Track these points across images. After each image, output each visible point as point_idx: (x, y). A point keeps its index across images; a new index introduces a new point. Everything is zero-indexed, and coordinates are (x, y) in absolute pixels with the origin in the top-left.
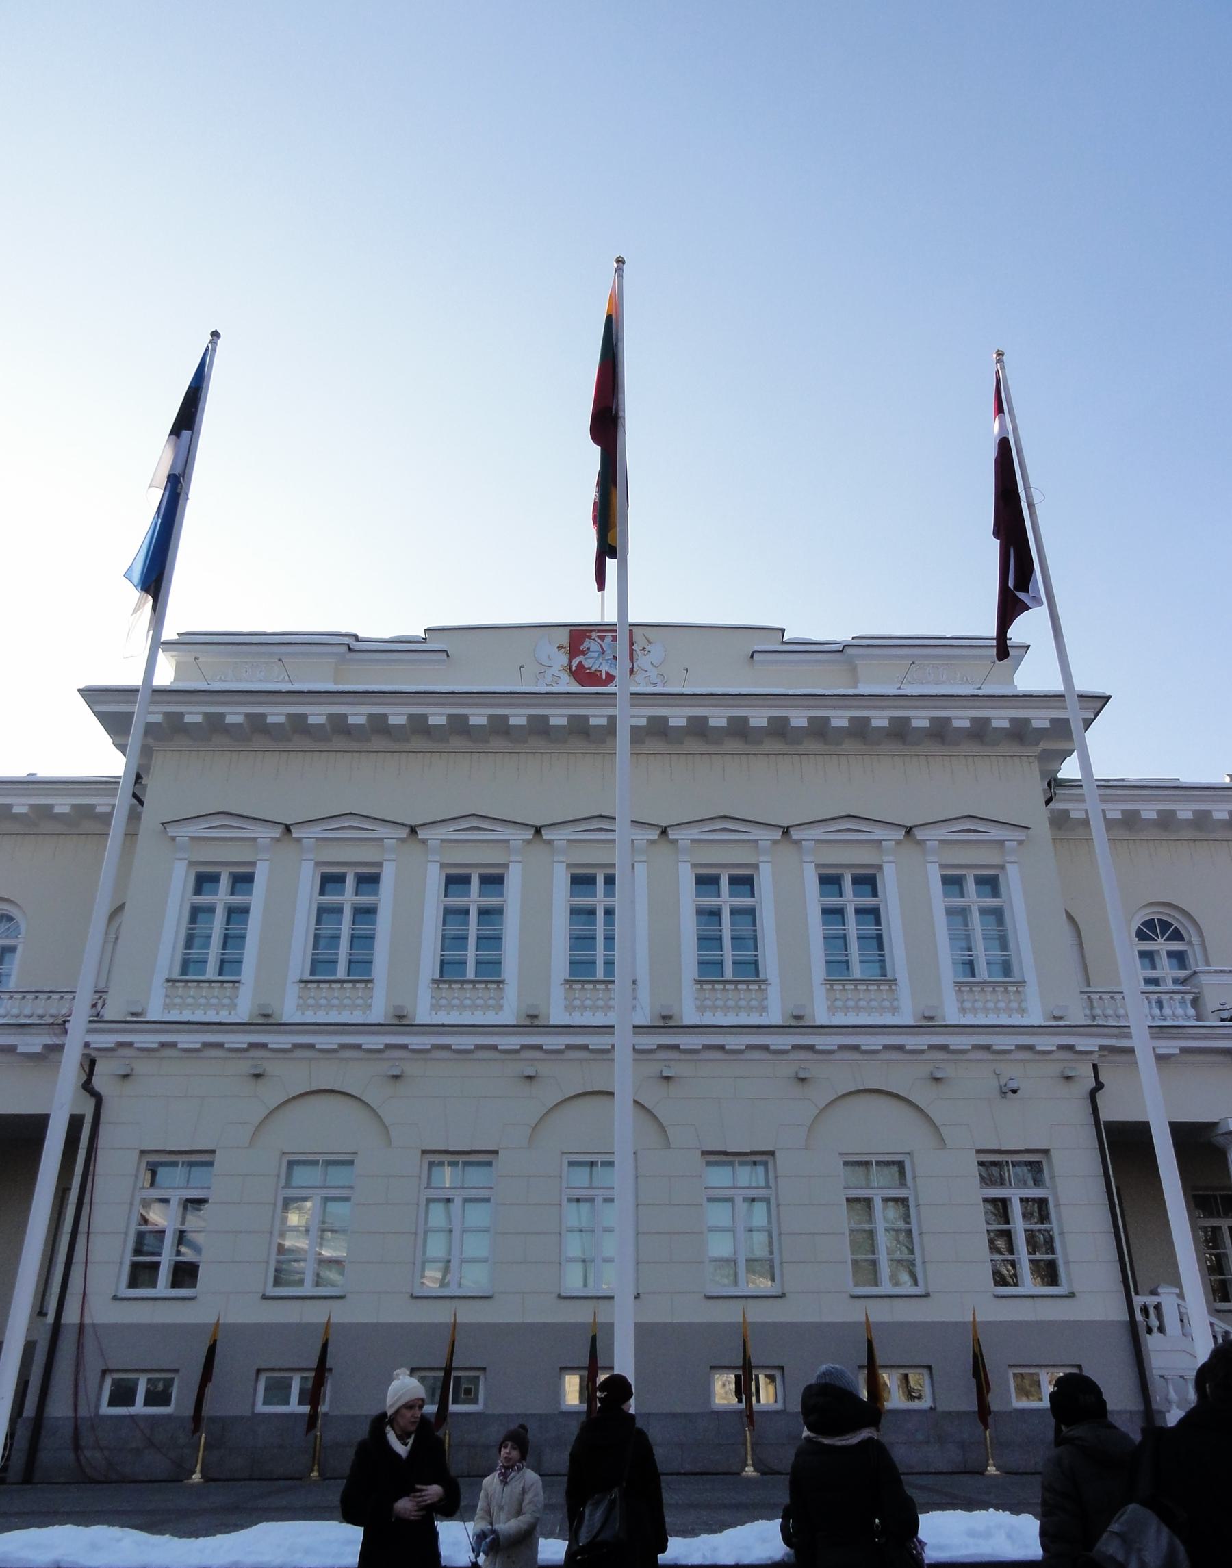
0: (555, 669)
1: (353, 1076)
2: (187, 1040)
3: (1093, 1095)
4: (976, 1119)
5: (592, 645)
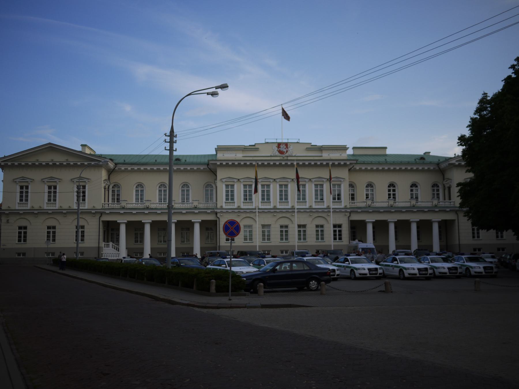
0: (276, 151)
1: (252, 215)
2: (230, 211)
3: (349, 217)
4: (333, 219)
5: (282, 146)
